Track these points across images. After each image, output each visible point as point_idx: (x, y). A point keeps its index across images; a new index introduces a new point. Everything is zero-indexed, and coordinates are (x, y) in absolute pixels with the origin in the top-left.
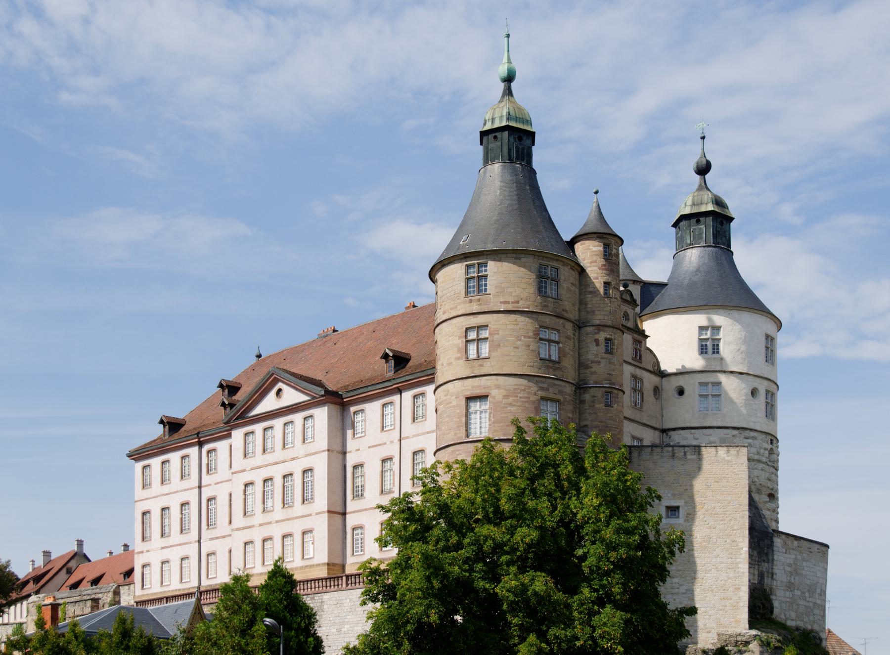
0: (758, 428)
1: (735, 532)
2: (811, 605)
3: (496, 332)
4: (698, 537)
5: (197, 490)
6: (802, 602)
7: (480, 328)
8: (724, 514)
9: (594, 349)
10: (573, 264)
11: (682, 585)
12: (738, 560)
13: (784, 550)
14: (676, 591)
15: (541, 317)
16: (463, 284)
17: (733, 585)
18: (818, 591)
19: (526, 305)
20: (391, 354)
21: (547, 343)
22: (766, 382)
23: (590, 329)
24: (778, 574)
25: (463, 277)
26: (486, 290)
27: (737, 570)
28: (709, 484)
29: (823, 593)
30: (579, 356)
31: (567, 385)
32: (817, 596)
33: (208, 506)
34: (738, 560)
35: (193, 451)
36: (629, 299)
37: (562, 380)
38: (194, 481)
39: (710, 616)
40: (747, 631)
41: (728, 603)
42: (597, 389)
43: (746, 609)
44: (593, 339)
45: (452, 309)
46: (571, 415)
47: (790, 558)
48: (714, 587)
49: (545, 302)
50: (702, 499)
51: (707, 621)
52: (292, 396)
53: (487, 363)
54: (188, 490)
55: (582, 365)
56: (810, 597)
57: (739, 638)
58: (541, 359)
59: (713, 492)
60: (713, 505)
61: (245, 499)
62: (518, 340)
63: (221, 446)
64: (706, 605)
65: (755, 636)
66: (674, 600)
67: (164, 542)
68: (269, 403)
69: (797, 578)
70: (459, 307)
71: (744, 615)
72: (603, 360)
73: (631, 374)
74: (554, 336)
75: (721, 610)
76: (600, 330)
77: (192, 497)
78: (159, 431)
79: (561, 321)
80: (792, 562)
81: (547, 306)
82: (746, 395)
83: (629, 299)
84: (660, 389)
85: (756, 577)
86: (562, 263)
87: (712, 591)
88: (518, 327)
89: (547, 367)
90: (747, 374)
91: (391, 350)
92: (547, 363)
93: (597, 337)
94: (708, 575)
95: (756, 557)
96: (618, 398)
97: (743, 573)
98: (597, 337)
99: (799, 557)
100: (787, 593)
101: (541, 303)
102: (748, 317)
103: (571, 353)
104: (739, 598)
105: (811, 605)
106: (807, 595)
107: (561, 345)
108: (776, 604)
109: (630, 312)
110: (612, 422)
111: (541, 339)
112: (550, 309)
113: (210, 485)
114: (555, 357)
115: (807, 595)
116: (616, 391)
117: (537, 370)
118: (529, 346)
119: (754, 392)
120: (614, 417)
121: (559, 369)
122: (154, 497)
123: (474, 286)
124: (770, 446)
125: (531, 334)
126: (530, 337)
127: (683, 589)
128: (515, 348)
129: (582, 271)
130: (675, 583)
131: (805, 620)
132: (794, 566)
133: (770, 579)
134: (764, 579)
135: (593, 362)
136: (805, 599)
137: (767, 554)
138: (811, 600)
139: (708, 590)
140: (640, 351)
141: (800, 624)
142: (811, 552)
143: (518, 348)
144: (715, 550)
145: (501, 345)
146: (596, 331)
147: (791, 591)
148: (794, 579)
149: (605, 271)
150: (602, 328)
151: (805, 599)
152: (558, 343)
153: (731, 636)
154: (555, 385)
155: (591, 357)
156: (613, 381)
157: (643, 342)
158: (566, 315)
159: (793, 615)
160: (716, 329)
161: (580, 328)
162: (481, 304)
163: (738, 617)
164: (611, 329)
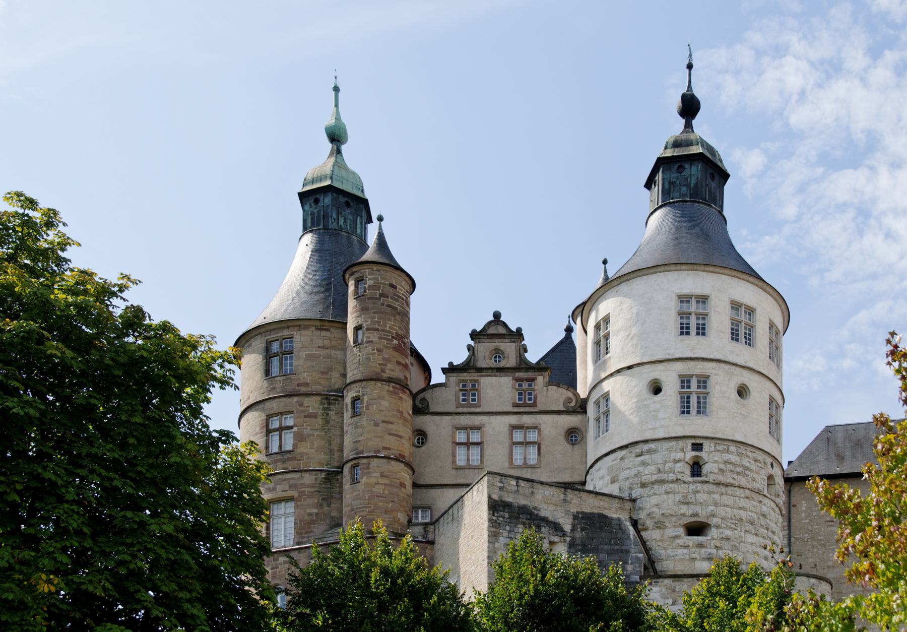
10: (318, 323)
31: (306, 475)
49: (272, 384)
74: (289, 421)
79: (296, 399)
81: (274, 388)
86: (296, 328)
96: (368, 468)
101: (267, 388)
107: (295, 429)
110: (359, 501)
116: (365, 461)
120: (361, 495)
121: (295, 458)
154: (285, 480)
156: (361, 448)
158: (303, 389)
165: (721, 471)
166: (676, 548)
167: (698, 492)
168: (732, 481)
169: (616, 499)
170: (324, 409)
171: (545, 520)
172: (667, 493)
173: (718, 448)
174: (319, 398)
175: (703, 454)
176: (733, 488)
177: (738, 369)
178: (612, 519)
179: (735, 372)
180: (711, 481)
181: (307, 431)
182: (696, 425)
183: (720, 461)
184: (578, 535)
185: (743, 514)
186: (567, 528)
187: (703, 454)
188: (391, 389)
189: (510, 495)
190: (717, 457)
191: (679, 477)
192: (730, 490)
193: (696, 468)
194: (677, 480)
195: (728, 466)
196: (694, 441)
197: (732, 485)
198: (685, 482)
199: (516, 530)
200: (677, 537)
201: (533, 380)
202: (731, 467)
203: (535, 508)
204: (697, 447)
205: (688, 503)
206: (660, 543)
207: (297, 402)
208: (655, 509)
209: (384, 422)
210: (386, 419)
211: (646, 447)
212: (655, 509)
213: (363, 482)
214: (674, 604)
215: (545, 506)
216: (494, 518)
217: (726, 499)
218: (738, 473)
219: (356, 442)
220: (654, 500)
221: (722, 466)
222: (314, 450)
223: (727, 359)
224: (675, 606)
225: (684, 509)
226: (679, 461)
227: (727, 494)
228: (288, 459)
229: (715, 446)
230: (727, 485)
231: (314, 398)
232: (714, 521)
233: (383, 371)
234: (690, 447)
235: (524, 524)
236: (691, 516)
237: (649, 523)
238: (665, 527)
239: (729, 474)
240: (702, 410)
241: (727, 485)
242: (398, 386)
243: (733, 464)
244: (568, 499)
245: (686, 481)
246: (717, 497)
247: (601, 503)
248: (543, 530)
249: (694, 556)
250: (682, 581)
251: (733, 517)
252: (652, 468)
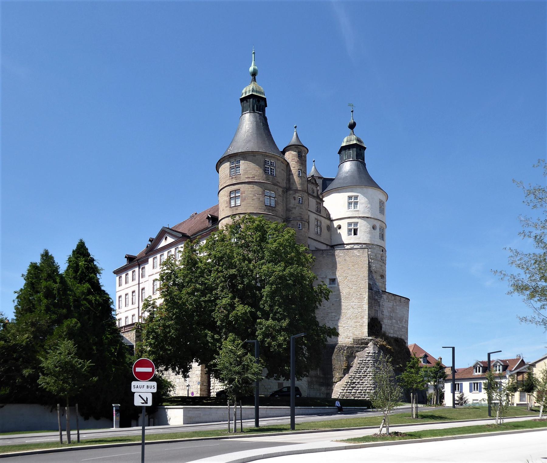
0: (376, 243)
1: (362, 290)
2: (401, 327)
3: (244, 192)
4: (344, 293)
5: (138, 285)
6: (395, 325)
7: (236, 191)
8: (357, 281)
9: (293, 201)
11: (336, 316)
12: (363, 303)
14: (334, 319)
15: (265, 185)
16: (229, 170)
17: (360, 316)
18: (404, 321)
19: (258, 179)
20: (210, 217)
21: (269, 197)
22: (380, 222)
23: (291, 192)
25: (229, 167)
26: (239, 172)
27: (362, 308)
28: (350, 267)
29: (407, 322)
30: (286, 205)
33: (142, 292)
34: (363, 303)
35: (137, 269)
36: (314, 182)
37: (276, 216)
38: (136, 282)
39: (350, 330)
40: (367, 338)
41: (358, 324)
42: (294, 221)
43: (367, 327)
44: (293, 197)
45: (224, 183)
47: (391, 304)
48: (352, 316)
50: (346, 275)
51: (348, 333)
52: (170, 240)
53: (240, 208)
54: (135, 285)
55: (288, 210)
56: (400, 323)
57: (363, 341)
58: (265, 205)
59: (351, 271)
60: (351, 277)
61: (153, 287)
62: (254, 196)
63: (147, 266)
64: (347, 326)
65: (371, 340)
66: (333, 323)
67: (126, 309)
68: (163, 243)
69: (394, 314)
70: (227, 182)
71: (365, 330)
72: (297, 207)
73: (315, 218)
75: (355, 328)
76: (296, 192)
77: (136, 288)
78: (125, 262)
79: (276, 187)
82: (370, 228)
83: (314, 182)
84: (330, 227)
87: (351, 318)
88: (254, 190)
89: (269, 209)
90: (371, 218)
91: (210, 215)
92: (269, 208)
93: (294, 196)
94: (349, 311)
97: (365, 310)
98: (294, 196)
99: (395, 304)
100: (389, 321)
102: (371, 191)
103: (281, 203)
104: (364, 322)
105: (401, 327)
106: (399, 322)
107: (276, 199)
108: (383, 326)
109: (315, 188)
111: (265, 196)
112: (270, 181)
113: (143, 283)
114: (273, 204)
115: (399, 322)
116: (304, 222)
117: (263, 211)
118: (259, 199)
119: (374, 228)
120: (303, 235)
121: (276, 211)
122: (123, 290)
123: (234, 171)
124: (382, 252)
125: (260, 193)
126: (260, 195)
127: (337, 318)
128: (252, 200)
129: (288, 164)
130: (333, 315)
131: (398, 334)
132: (392, 308)
135: (292, 208)
136: (397, 324)
138: (400, 324)
139: (349, 318)
140: (320, 208)
141: (396, 336)
142: (401, 302)
143: (254, 200)
144: (352, 299)
145: (246, 198)
146: (294, 193)
147: (391, 320)
148: (393, 314)
149: (299, 164)
150: (297, 191)
151: (397, 324)
152: (274, 198)
153: (359, 340)
154: (273, 218)
155: (291, 205)
157: (322, 204)
158: (278, 184)
159: (392, 331)
160: (356, 197)
161: (287, 192)
162: (237, 179)
163: (363, 331)
164: (301, 192)
181: (279, 202)
207: (277, 188)
213: (303, 230)
219: (301, 214)
222: (281, 210)
228: (274, 210)
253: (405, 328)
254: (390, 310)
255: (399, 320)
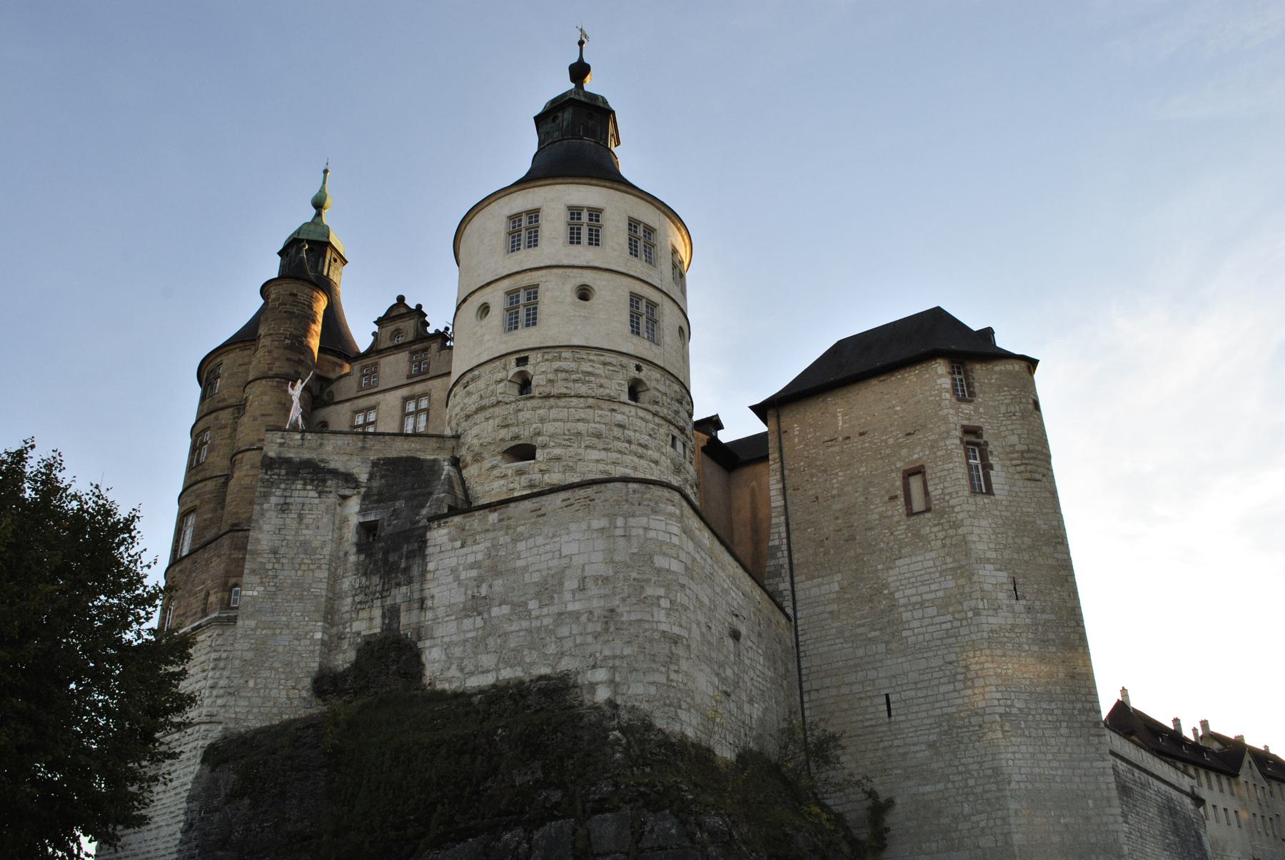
13: (458, 544)
18: (570, 584)
24: (437, 596)
32: (568, 596)
46: (210, 516)
80: (480, 557)
85: (378, 622)
95: (376, 585)
100: (468, 623)
106: (533, 605)
133: (416, 612)
134: (399, 617)
137: (407, 570)
147: (480, 614)
148: (490, 586)
154: (194, 491)
158: (221, 405)
165: (551, 381)
166: (493, 481)
167: (520, 410)
168: (564, 391)
169: (434, 439)
170: (234, 418)
171: (335, 473)
172: (487, 419)
173: (546, 357)
174: (231, 409)
175: (529, 368)
176: (568, 399)
177: (576, 270)
178: (425, 461)
179: (571, 275)
180: (537, 395)
182: (525, 338)
183: (549, 370)
184: (375, 484)
185: (581, 427)
186: (363, 477)
187: (529, 368)
188: (275, 384)
189: (292, 450)
190: (543, 367)
191: (500, 399)
192: (562, 402)
193: (525, 384)
194: (499, 402)
195: (559, 375)
196: (517, 356)
197: (565, 396)
198: (507, 403)
199: (293, 487)
200: (493, 467)
201: (425, 350)
202: (564, 375)
203: (323, 461)
204: (522, 361)
205: (507, 426)
206: (477, 480)
208: (475, 441)
209: (263, 415)
210: (264, 412)
211: (469, 376)
212: (475, 441)
214: (463, 546)
215: (336, 458)
216: (267, 477)
217: (554, 413)
218: (575, 381)
220: (475, 431)
221: (551, 376)
223: (561, 264)
224: (465, 549)
225: (503, 433)
226: (501, 381)
227: (557, 407)
229: (543, 357)
230: (559, 396)
231: (228, 411)
232: (539, 440)
233: (270, 369)
234: (514, 364)
235: (304, 479)
236: (511, 439)
237: (469, 459)
238: (483, 459)
239: (560, 383)
240: (532, 320)
241: (559, 396)
242: (283, 380)
243: (567, 372)
244: (368, 445)
245: (508, 401)
246: (541, 412)
247: (413, 445)
248: (329, 483)
249: (511, 486)
250: (474, 515)
251: (567, 432)
252: (475, 397)
253: (584, 618)
254: (474, 573)
255: (538, 595)
